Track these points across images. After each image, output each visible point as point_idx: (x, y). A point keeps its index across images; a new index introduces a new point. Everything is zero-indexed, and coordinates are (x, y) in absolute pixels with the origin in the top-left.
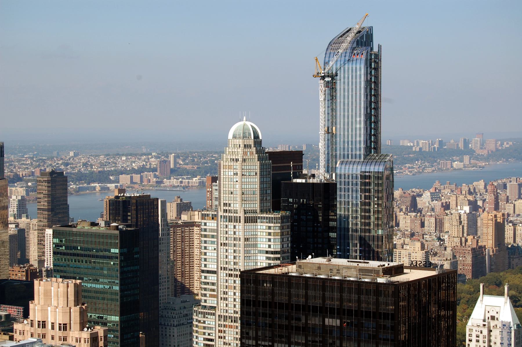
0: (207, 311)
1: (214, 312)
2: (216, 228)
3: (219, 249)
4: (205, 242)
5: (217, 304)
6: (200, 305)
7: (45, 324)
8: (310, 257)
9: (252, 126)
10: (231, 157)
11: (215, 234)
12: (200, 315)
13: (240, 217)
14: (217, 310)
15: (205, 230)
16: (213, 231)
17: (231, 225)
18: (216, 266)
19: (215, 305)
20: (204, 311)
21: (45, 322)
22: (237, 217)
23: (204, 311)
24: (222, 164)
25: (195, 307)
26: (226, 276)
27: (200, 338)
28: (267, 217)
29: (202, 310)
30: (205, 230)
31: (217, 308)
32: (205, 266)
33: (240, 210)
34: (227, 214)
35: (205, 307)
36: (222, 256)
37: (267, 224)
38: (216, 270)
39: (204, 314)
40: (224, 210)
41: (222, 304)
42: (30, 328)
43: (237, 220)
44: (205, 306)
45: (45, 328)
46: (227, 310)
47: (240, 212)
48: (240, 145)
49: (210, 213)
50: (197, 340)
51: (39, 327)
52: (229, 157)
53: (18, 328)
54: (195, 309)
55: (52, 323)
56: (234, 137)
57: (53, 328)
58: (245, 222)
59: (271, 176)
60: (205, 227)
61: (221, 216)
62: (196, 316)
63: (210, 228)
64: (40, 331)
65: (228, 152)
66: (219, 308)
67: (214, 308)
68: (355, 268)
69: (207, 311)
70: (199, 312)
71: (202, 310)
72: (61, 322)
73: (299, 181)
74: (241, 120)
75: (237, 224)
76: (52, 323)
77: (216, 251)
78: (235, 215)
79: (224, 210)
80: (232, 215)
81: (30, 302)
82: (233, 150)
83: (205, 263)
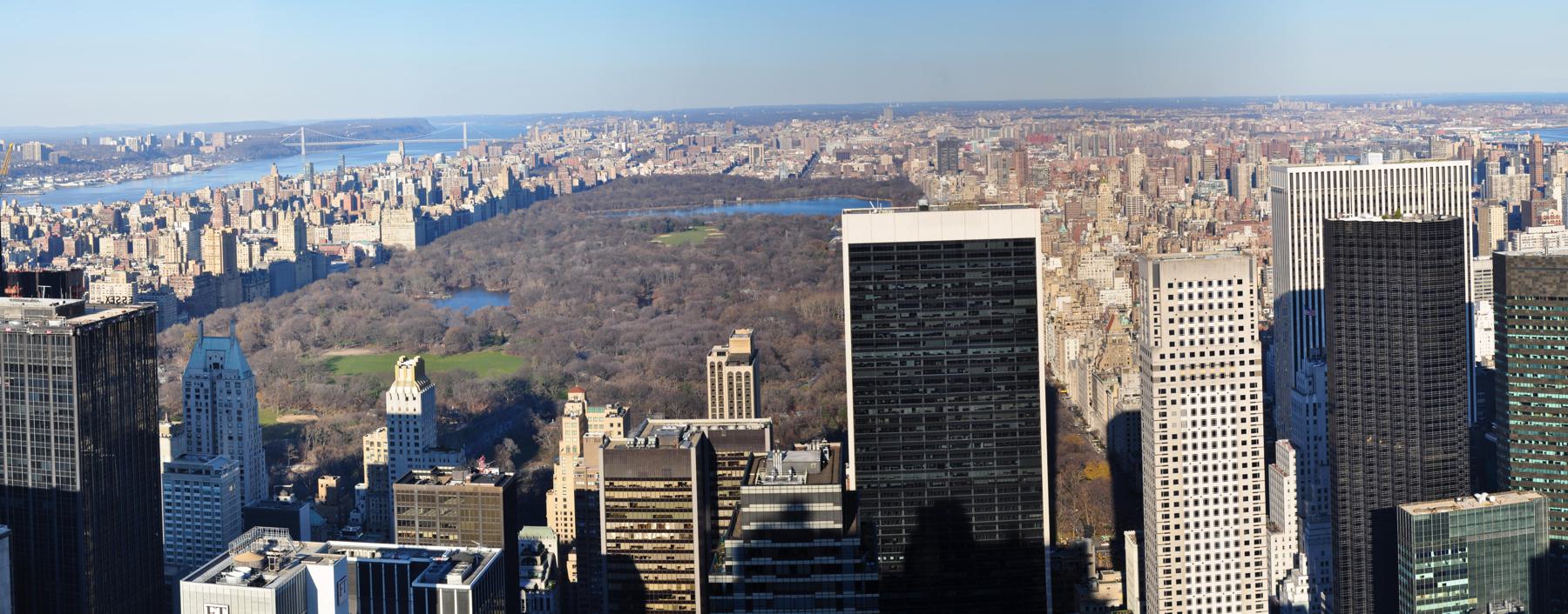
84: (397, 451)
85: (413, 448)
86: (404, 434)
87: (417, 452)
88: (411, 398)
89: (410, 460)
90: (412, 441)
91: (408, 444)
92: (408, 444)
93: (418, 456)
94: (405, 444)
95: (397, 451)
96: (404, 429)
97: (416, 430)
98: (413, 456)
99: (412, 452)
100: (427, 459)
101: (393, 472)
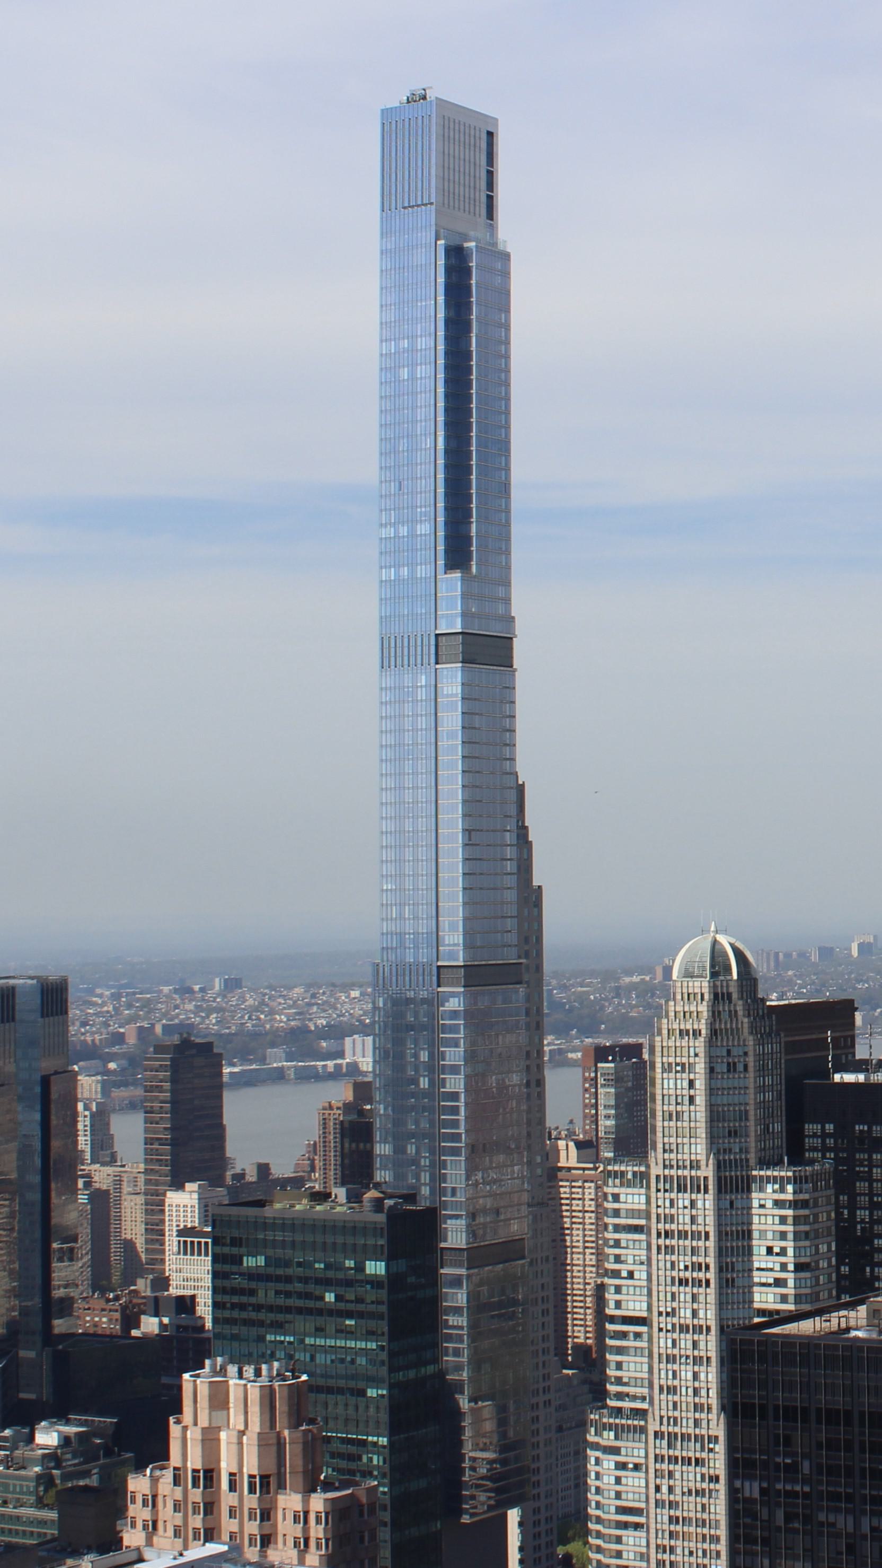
0: (624, 1421)
1: (642, 1423)
2: (643, 1207)
3: (654, 1262)
4: (617, 1244)
6: (605, 1406)
7: (212, 1477)
9: (732, 945)
10: (682, 1027)
11: (643, 1222)
12: (605, 1433)
13: (706, 1178)
14: (650, 1420)
15: (616, 1213)
16: (636, 1214)
17: (684, 1200)
18: (645, 1306)
20: (617, 1421)
21: (212, 1471)
22: (698, 1178)
23: (617, 1421)
25: (591, 1413)
27: (606, 1493)
28: (775, 1178)
29: (611, 1420)
30: (616, 1213)
31: (650, 1415)
32: (618, 1304)
33: (708, 1160)
34: (673, 1172)
35: (619, 1411)
36: (662, 1279)
38: (645, 1314)
39: (619, 1431)
42: (173, 1490)
43: (699, 1187)
47: (707, 1165)
48: (702, 995)
49: (629, 1168)
50: (598, 1498)
52: (676, 1026)
53: (138, 1489)
54: (592, 1416)
55: (231, 1474)
56: (688, 974)
59: (783, 1072)
60: (616, 1206)
61: (658, 1177)
62: (596, 1434)
63: (629, 1206)
65: (673, 1014)
66: (657, 1413)
67: (641, 1414)
69: (624, 1421)
70: (604, 1424)
71: (611, 1420)
72: (255, 1472)
73: (849, 1078)
74: (704, 931)
75: (700, 1196)
76: (231, 1474)
77: (644, 1267)
78: (693, 1173)
80: (686, 1173)
81: (172, 1420)
82: (686, 1009)
83: (618, 1297)
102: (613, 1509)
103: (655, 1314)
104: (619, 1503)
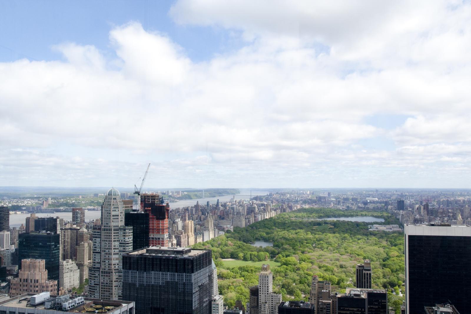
5: (101, 266)
8: (151, 246)
14: (100, 269)
19: (99, 267)
24: (103, 206)
26: (105, 254)
37: (123, 232)
40: (104, 226)
41: (103, 267)
44: (95, 267)
45: (27, 282)
46: (105, 269)
51: (24, 281)
57: (31, 282)
58: (114, 231)
64: (25, 283)
67: (99, 268)
68: (172, 251)
79: (104, 226)
84: (262, 293)
85: (266, 293)
86: (264, 288)
87: (268, 294)
88: (266, 277)
89: (265, 296)
90: (266, 290)
91: (265, 291)
92: (265, 291)
93: (268, 295)
94: (264, 291)
95: (262, 293)
96: (264, 287)
97: (268, 287)
98: (266, 295)
99: (266, 294)
100: (271, 296)
101: (260, 300)
102: (93, 284)
103: (102, 251)
104: (94, 283)
